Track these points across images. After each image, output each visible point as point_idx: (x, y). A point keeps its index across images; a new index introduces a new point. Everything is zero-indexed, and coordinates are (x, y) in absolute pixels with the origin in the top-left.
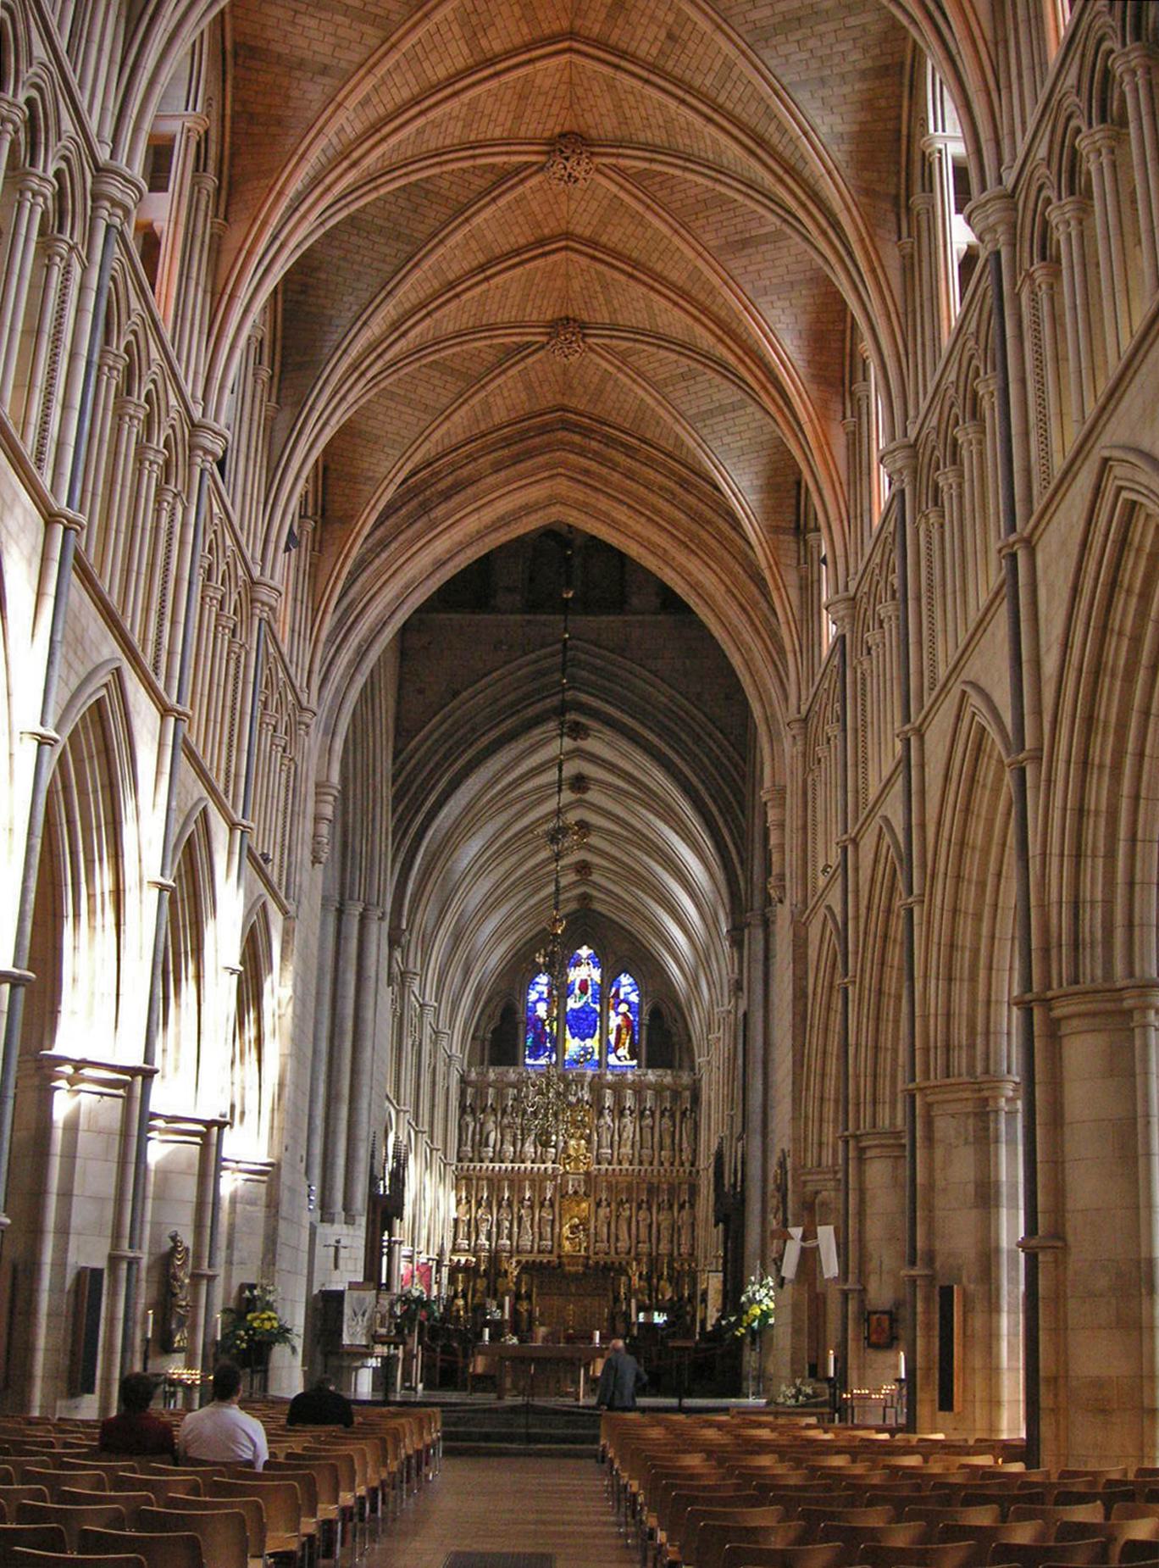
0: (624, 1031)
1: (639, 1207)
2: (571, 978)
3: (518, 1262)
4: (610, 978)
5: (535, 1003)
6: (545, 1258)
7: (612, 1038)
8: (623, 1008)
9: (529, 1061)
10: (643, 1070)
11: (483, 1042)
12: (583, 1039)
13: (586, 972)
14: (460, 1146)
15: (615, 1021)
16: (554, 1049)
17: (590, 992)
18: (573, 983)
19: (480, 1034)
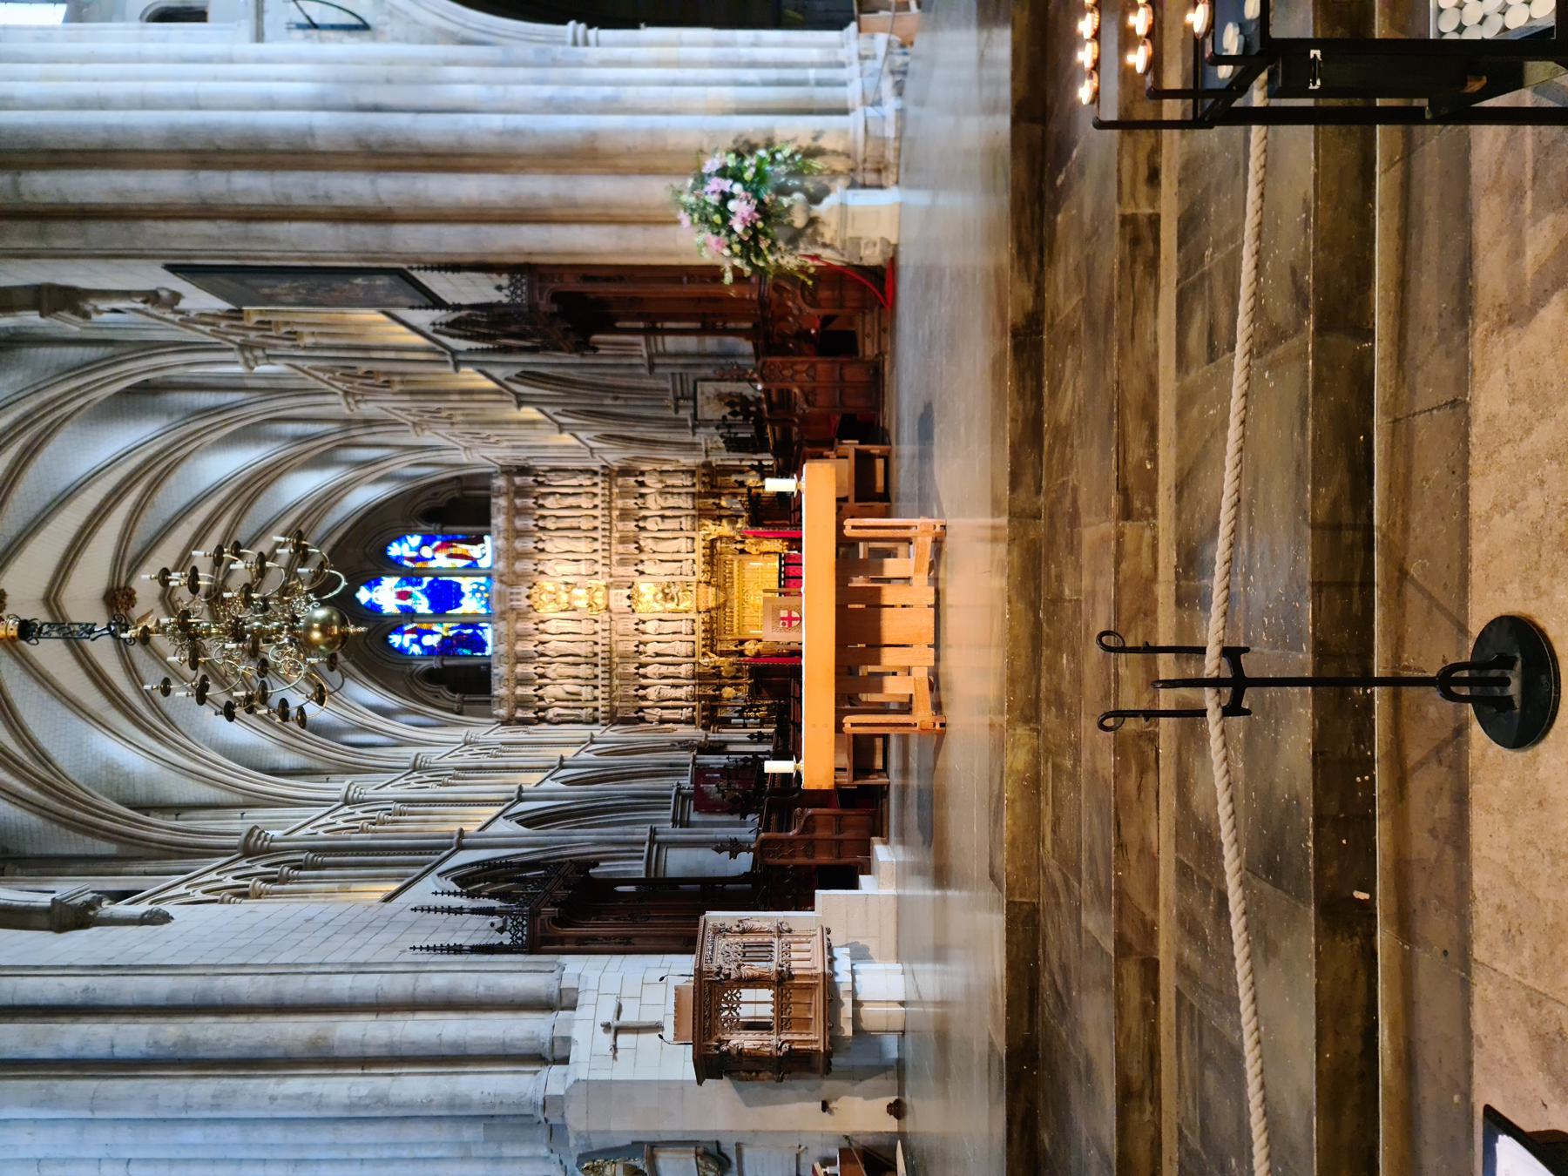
0: (452, 551)
1: (643, 529)
2: (396, 611)
3: (704, 654)
4: (394, 566)
5: (423, 647)
6: (699, 627)
7: (461, 563)
8: (426, 552)
9: (489, 651)
10: (493, 528)
11: (465, 702)
12: (462, 595)
13: (385, 595)
14: (581, 722)
15: (441, 561)
16: (474, 626)
17: (409, 588)
18: (401, 607)
19: (455, 706)
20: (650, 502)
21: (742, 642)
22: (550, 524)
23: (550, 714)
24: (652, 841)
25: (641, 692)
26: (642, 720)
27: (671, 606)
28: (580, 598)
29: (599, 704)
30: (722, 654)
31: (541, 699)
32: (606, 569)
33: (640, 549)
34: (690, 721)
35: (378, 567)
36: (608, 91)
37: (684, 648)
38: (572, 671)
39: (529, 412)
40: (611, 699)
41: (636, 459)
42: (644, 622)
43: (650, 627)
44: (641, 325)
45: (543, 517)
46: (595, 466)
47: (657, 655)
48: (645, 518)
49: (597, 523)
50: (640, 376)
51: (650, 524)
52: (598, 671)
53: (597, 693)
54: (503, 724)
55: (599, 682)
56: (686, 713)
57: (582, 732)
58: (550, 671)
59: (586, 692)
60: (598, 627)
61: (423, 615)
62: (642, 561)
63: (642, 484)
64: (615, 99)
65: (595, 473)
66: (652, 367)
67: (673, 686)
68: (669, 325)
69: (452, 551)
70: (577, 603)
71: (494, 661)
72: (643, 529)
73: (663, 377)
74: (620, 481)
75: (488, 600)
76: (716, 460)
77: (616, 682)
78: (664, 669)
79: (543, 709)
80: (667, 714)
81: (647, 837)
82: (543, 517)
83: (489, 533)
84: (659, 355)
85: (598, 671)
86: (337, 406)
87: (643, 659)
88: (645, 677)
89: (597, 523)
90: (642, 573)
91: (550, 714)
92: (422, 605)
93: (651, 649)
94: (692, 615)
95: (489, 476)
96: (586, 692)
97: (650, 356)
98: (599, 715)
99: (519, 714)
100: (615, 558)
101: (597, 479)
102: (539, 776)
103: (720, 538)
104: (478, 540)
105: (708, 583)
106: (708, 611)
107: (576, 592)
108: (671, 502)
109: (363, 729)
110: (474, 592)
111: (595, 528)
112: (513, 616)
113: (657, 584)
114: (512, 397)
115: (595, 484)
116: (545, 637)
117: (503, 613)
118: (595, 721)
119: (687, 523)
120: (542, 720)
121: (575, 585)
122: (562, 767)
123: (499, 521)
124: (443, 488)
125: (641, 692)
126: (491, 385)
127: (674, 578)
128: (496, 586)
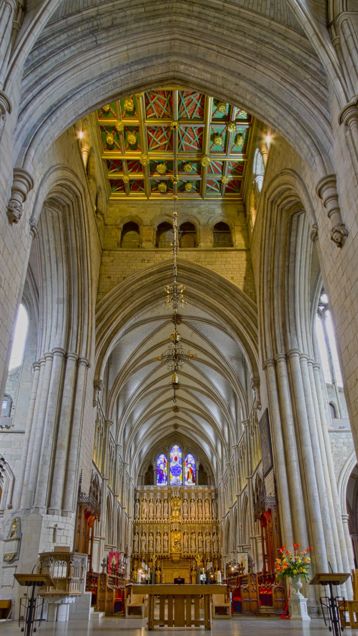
3: (156, 556)
6: (166, 554)
20: (208, 537)
21: (160, 570)
22: (200, 504)
23: (137, 504)
24: (101, 538)
25: (144, 534)
26: (135, 534)
27: (173, 544)
28: (175, 514)
29: (141, 520)
30: (156, 562)
31: (142, 501)
32: (185, 522)
33: (192, 533)
34: (134, 552)
35: (185, 451)
36: (330, 526)
37: (159, 549)
38: (151, 511)
39: (235, 499)
40: (142, 524)
41: (222, 532)
42: (167, 535)
43: (166, 537)
44: (264, 535)
45: (202, 502)
46: (220, 519)
47: (156, 540)
48: (202, 535)
49: (200, 519)
50: (249, 534)
51: (200, 537)
52: (151, 520)
53: (144, 519)
54: (135, 489)
55: (148, 520)
56: (136, 550)
57: (132, 514)
58: (151, 504)
59: (144, 516)
60: (166, 519)
61: (170, 465)
62: (188, 534)
63: (213, 534)
64: (327, 528)
65: (217, 519)
66: (252, 538)
67: (146, 545)
68: (265, 543)
69: (190, 473)
70: (174, 512)
71: (155, 486)
72: (199, 535)
73: (249, 542)
74: (214, 527)
75: (175, 484)
76: (223, 559)
77: (147, 525)
78: (151, 542)
79: (139, 501)
80: (136, 543)
81: (102, 536)
82: (202, 502)
83: (196, 485)
84: (256, 541)
85: (151, 520)
86: (234, 443)
87: (155, 535)
88: (149, 535)
89: (200, 519)
90: (184, 534)
91: (137, 504)
92: (173, 464)
93: (158, 537)
94: (169, 552)
95: (214, 485)
96: (144, 516)
97: (255, 538)
98: (137, 519)
99: (138, 494)
100: (189, 525)
101: (215, 519)
102: (120, 501)
103: (196, 562)
104: (194, 481)
105: (180, 557)
106: (171, 557)
107: (178, 512)
108: (208, 544)
109: (136, 448)
110: (177, 480)
111: (198, 519)
112: (169, 492)
113: (180, 539)
114: (239, 494)
115: (213, 519)
116: (162, 502)
117: (171, 489)
118: (135, 519)
119: (200, 550)
120: (136, 500)
121: (180, 511)
122: (122, 508)
123: (200, 488)
124: (210, 470)
125: (144, 534)
126: (243, 487)
127: (182, 546)
128: (179, 487)
